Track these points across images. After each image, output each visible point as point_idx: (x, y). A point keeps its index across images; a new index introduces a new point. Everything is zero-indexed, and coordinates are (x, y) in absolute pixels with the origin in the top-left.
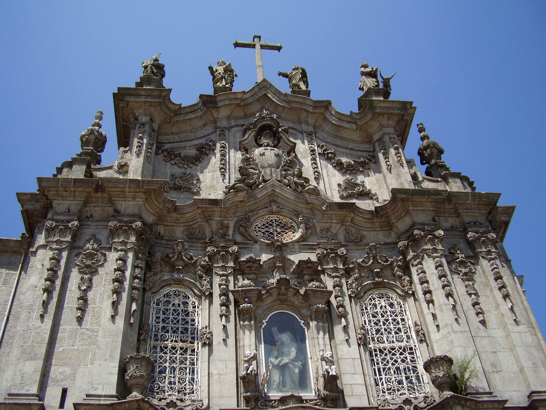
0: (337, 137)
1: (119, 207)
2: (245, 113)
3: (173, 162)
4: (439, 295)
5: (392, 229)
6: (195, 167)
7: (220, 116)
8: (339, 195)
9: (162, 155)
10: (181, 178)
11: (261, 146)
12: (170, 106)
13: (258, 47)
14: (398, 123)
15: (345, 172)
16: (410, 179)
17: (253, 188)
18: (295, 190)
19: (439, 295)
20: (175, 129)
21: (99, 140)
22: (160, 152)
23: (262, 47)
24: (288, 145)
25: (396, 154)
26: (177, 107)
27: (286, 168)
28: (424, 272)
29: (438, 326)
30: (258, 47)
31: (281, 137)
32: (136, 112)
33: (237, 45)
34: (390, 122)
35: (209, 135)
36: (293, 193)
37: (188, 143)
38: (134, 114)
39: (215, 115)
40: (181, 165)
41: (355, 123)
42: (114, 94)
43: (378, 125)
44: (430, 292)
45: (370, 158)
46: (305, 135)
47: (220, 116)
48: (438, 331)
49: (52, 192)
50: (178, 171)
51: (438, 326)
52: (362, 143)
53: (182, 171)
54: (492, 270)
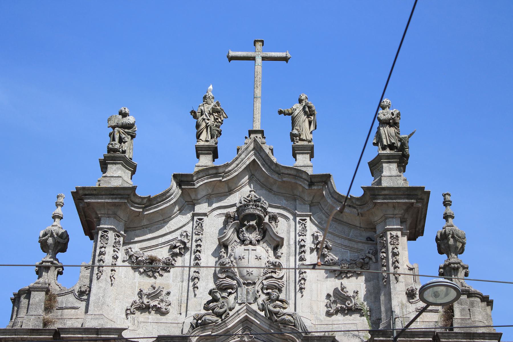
3: (142, 270)
6: (165, 274)
7: (199, 196)
8: (326, 309)
9: (130, 260)
10: (148, 296)
11: (243, 242)
12: (137, 201)
13: (259, 60)
14: (407, 210)
15: (339, 275)
16: (405, 298)
17: (223, 317)
20: (145, 222)
21: (59, 242)
22: (128, 258)
23: (264, 59)
25: (393, 263)
26: (145, 200)
27: (269, 275)
30: (259, 60)
31: (267, 229)
32: (98, 212)
33: (231, 59)
34: (396, 212)
35: (184, 226)
36: (267, 322)
37: (160, 239)
38: (97, 214)
39: (193, 197)
40: (150, 273)
41: (355, 208)
42: (73, 193)
43: (382, 215)
45: (370, 255)
46: (298, 219)
47: (199, 196)
50: (146, 283)
52: (366, 229)
53: (152, 280)
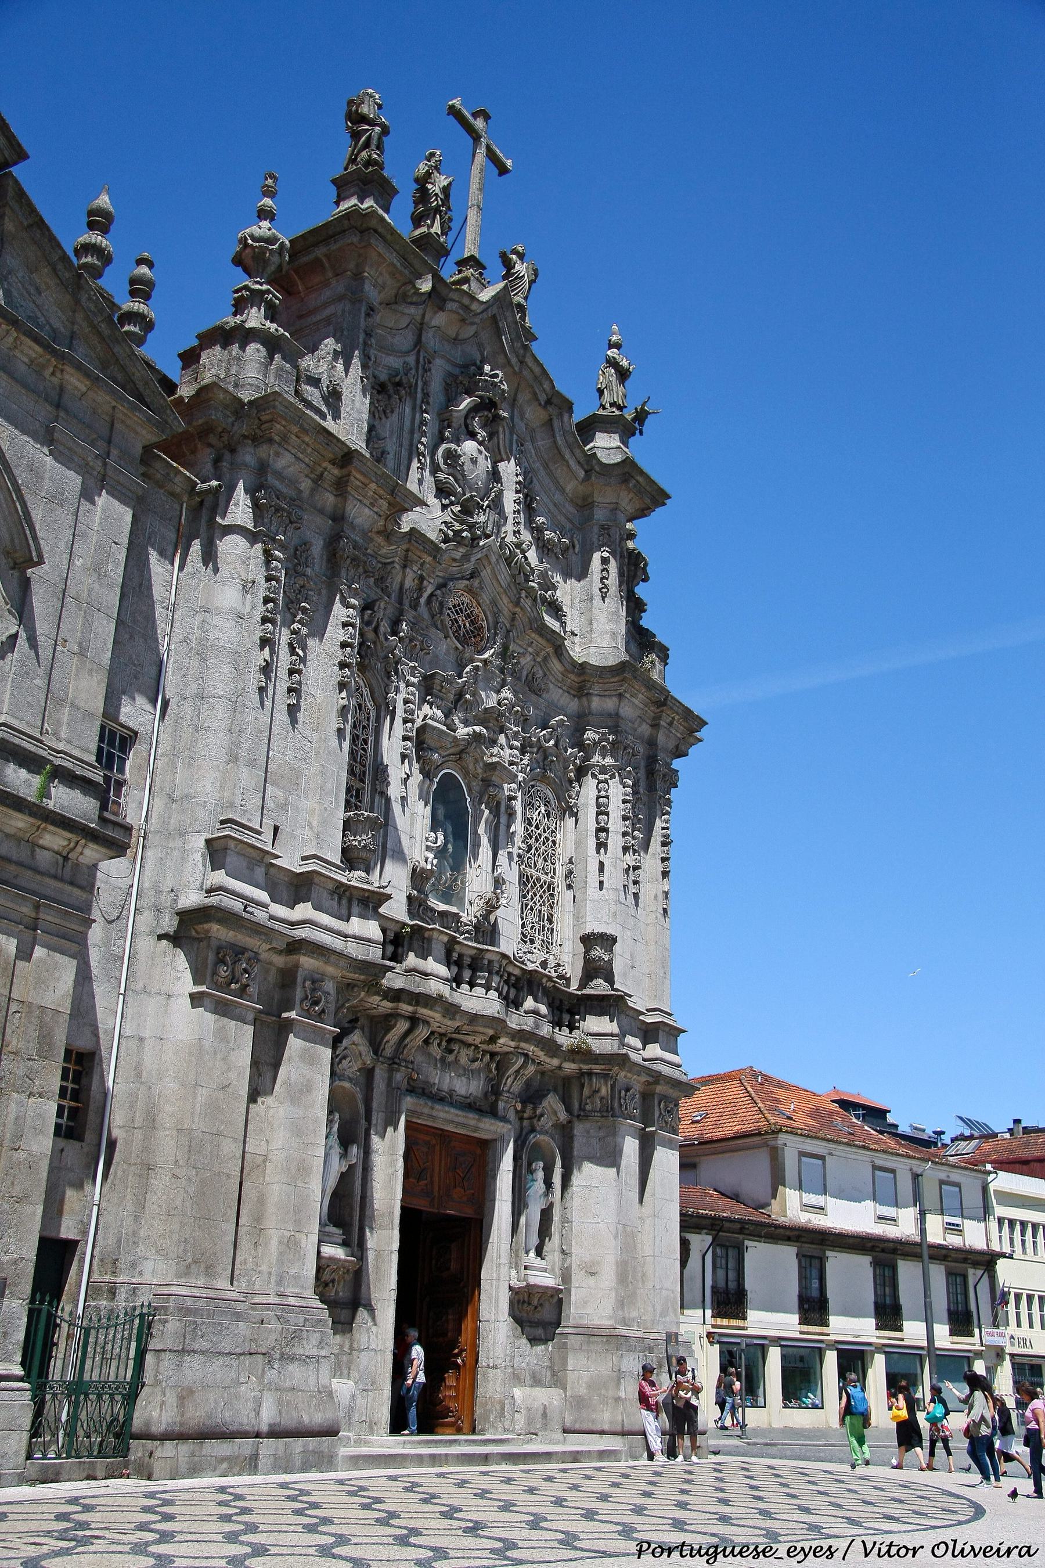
0: (546, 466)
1: (348, 509)
2: (457, 334)
4: (615, 842)
5: (579, 698)
18: (513, 576)
19: (615, 842)
24: (500, 453)
28: (607, 797)
29: (601, 883)
31: (497, 432)
32: (367, 269)
44: (605, 830)
48: (601, 889)
49: (278, 426)
51: (601, 883)
54: (663, 829)
